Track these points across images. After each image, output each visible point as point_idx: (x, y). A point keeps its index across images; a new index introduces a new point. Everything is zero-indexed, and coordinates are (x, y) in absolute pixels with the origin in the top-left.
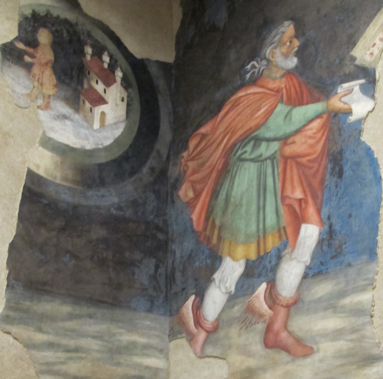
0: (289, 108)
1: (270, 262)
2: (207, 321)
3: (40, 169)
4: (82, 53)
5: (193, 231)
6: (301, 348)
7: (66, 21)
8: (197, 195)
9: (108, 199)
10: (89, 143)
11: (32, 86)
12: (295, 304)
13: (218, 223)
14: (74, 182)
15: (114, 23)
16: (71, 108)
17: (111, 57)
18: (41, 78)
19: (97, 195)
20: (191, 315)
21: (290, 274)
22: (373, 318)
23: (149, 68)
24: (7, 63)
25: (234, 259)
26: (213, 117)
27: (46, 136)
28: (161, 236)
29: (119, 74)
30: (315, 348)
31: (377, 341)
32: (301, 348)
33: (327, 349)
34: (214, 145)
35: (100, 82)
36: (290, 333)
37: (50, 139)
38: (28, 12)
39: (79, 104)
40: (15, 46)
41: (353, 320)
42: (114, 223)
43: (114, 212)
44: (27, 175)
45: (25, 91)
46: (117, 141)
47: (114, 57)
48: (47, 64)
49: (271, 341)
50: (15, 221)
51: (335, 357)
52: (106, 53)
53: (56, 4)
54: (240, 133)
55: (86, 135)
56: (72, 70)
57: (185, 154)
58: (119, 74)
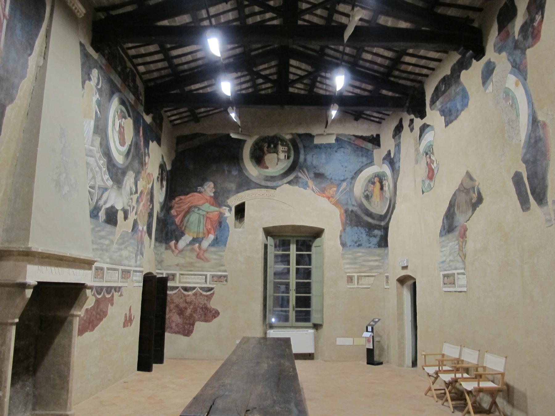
6: (207, 260)
12: (205, 251)
13: (185, 224)
21: (205, 244)
25: (189, 235)
32: (207, 260)
49: (198, 256)
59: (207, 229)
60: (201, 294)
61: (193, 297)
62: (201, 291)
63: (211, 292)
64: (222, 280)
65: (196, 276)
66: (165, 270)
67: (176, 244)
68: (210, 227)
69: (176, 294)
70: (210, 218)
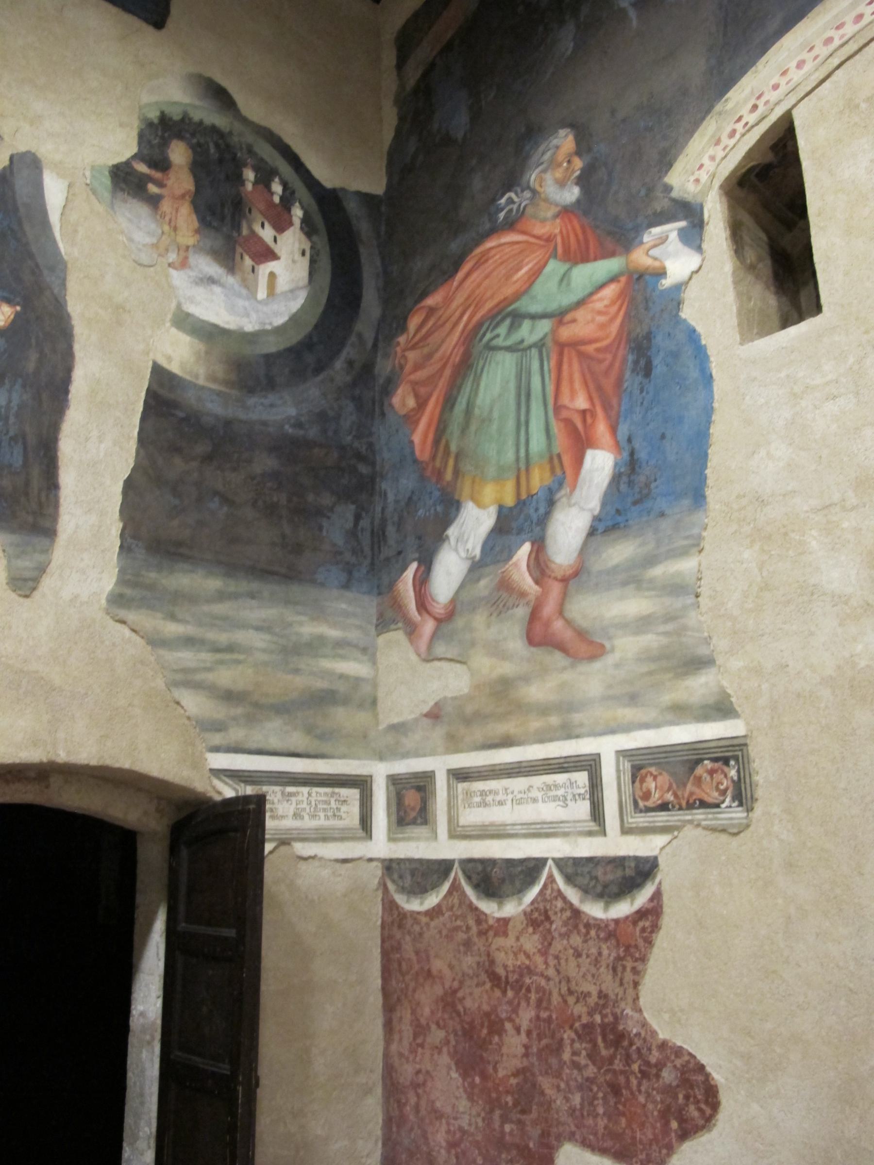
0: (566, 266)
1: (537, 510)
2: (438, 603)
3: (173, 363)
4: (239, 179)
5: (415, 461)
6: (586, 646)
7: (214, 129)
8: (422, 404)
9: (280, 410)
10: (250, 322)
11: (160, 231)
13: (453, 448)
14: (227, 383)
15: (291, 132)
16: (222, 266)
17: (285, 185)
18: (173, 218)
19: (262, 404)
20: (411, 593)
22: (699, 599)
23: (345, 204)
24: (120, 194)
25: (480, 505)
26: (446, 280)
27: (182, 311)
28: (363, 469)
29: (297, 213)
30: (608, 646)
31: (706, 634)
32: (586, 646)
33: (627, 647)
34: (448, 326)
35: (266, 225)
36: (568, 622)
37: (188, 315)
38: (153, 115)
39: (234, 260)
40: (132, 168)
41: (668, 601)
42: (290, 448)
43: (290, 431)
44: (152, 372)
45: (149, 240)
46: (294, 319)
47: (290, 185)
48: (183, 196)
49: (538, 635)
50: (133, 445)
51: (639, 660)
52: (277, 180)
53: (197, 103)
54: (489, 305)
55: (245, 309)
56: (223, 205)
57: (402, 339)
58: (297, 213)
59: (568, 422)
60: (576, 913)
61: (531, 943)
62: (573, 895)
63: (642, 898)
64: (713, 796)
65: (539, 781)
66: (381, 758)
67: (422, 582)
68: (581, 402)
69: (435, 912)
70: (575, 344)
